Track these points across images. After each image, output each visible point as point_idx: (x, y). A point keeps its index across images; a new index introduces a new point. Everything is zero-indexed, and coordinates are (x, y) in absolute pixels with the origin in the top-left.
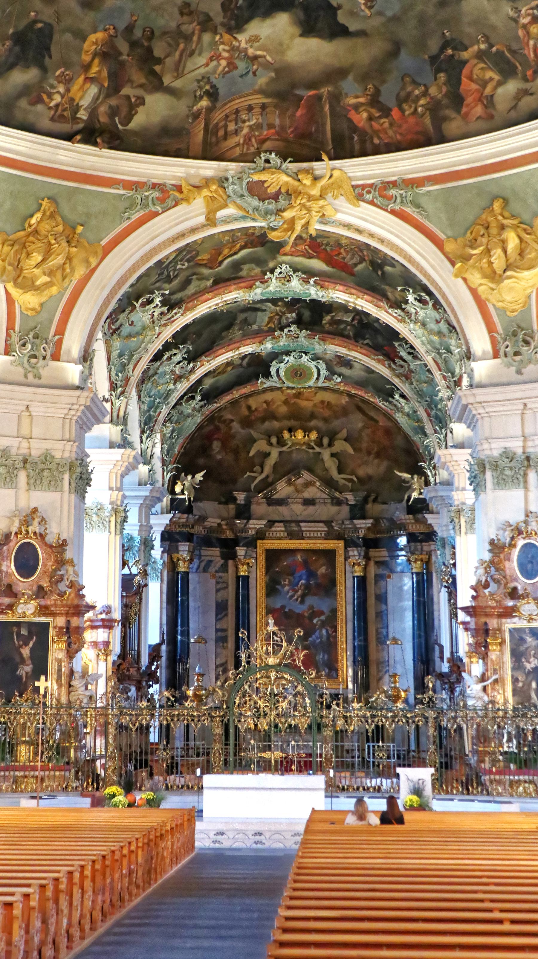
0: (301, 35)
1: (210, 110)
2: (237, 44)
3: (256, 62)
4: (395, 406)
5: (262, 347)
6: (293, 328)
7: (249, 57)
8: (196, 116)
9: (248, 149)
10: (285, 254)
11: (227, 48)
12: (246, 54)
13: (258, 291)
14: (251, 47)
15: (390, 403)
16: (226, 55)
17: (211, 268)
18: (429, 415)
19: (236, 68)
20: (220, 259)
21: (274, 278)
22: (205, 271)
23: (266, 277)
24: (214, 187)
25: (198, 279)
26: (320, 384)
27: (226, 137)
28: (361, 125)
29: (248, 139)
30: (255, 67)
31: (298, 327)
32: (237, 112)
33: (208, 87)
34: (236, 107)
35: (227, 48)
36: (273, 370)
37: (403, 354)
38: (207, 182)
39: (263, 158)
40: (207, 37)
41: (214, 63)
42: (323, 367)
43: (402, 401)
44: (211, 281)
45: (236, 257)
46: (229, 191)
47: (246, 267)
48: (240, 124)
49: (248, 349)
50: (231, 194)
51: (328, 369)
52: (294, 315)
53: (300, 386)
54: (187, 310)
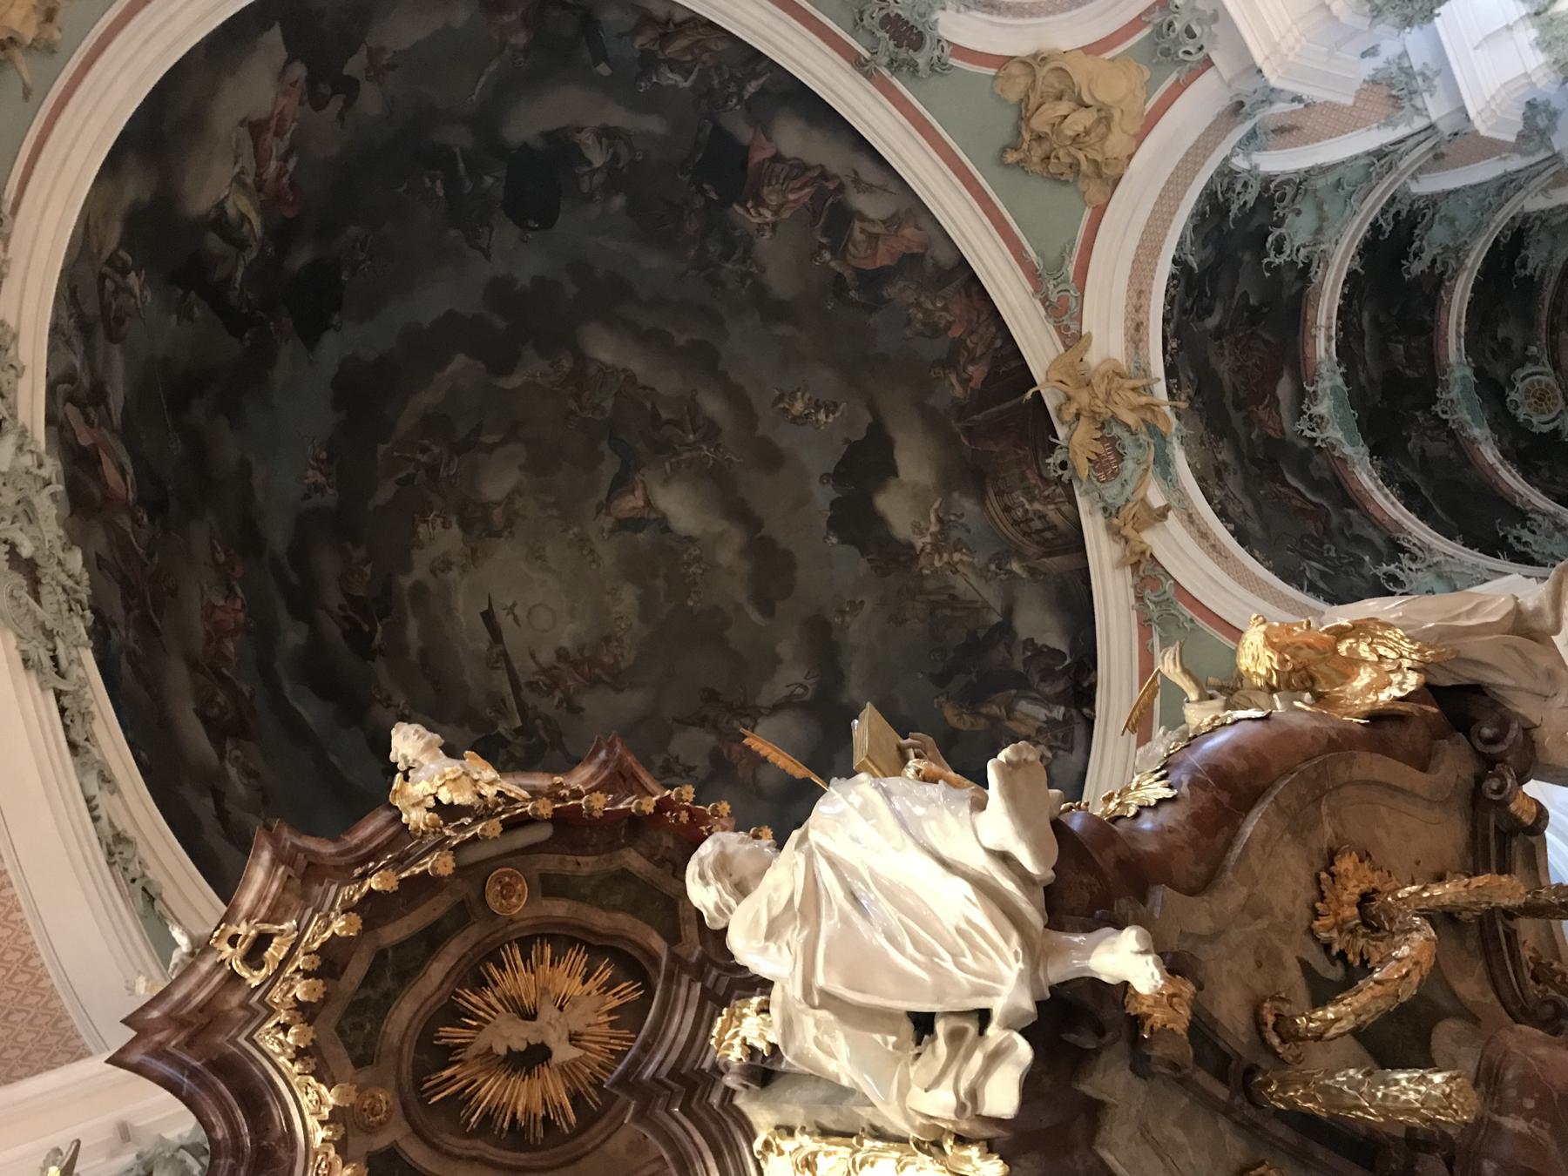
0: (897, 475)
1: (1021, 557)
2: (929, 547)
3: (946, 518)
4: (1543, 272)
5: (1481, 439)
6: (1437, 408)
7: (942, 529)
8: (1033, 572)
9: (1060, 496)
10: (1282, 431)
11: (937, 557)
12: (940, 532)
13: (1348, 450)
14: (928, 529)
15: (1542, 278)
16: (946, 557)
17: (1328, 515)
18: (1502, 206)
19: (959, 540)
20: (1311, 507)
21: (1324, 436)
22: (1335, 520)
23: (1324, 446)
24: (1116, 521)
25: (1350, 525)
26: (1548, 369)
27: (1053, 527)
28: (985, 369)
29: (1048, 500)
30: (953, 518)
31: (1435, 404)
32: (1016, 523)
33: (993, 567)
34: (1009, 526)
35: (937, 557)
36: (1546, 429)
37: (1417, 267)
38: (1115, 532)
39: (1060, 472)
40: (930, 585)
41: (960, 567)
42: (1521, 373)
43: (1531, 264)
44: (1351, 511)
45: (1303, 490)
46: (1120, 502)
47: (1316, 474)
48: (1031, 515)
49: (1490, 454)
50: (1124, 497)
51: (1522, 366)
52: (1418, 413)
53: (1559, 391)
54: (1399, 526)
